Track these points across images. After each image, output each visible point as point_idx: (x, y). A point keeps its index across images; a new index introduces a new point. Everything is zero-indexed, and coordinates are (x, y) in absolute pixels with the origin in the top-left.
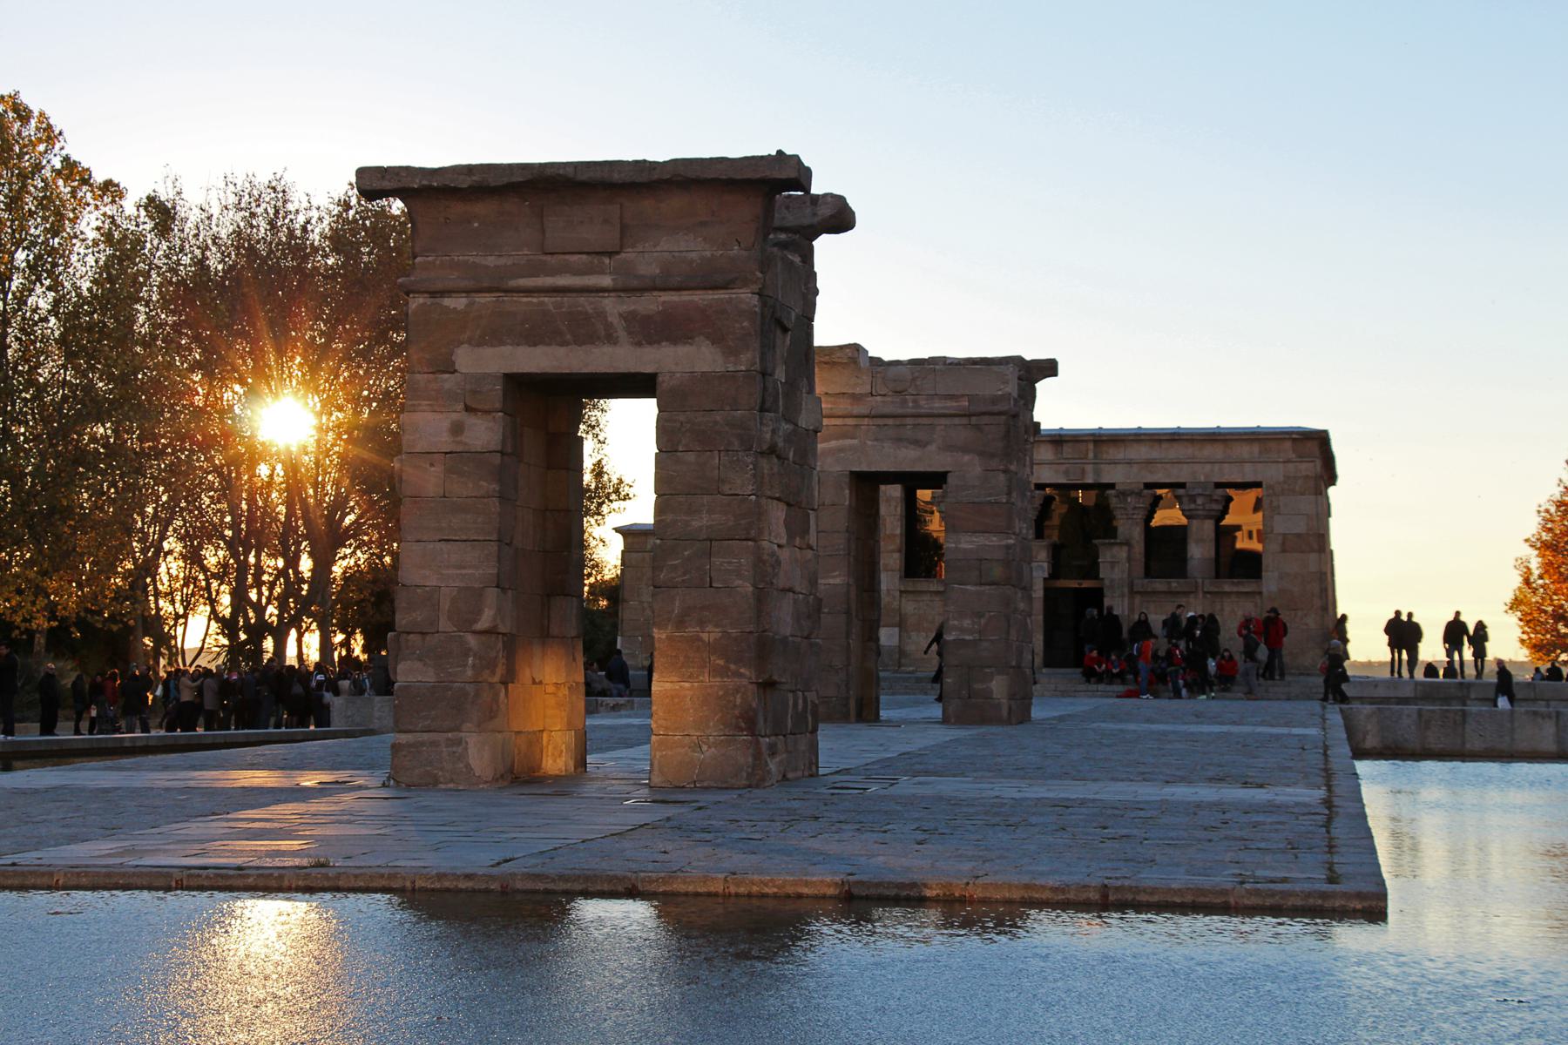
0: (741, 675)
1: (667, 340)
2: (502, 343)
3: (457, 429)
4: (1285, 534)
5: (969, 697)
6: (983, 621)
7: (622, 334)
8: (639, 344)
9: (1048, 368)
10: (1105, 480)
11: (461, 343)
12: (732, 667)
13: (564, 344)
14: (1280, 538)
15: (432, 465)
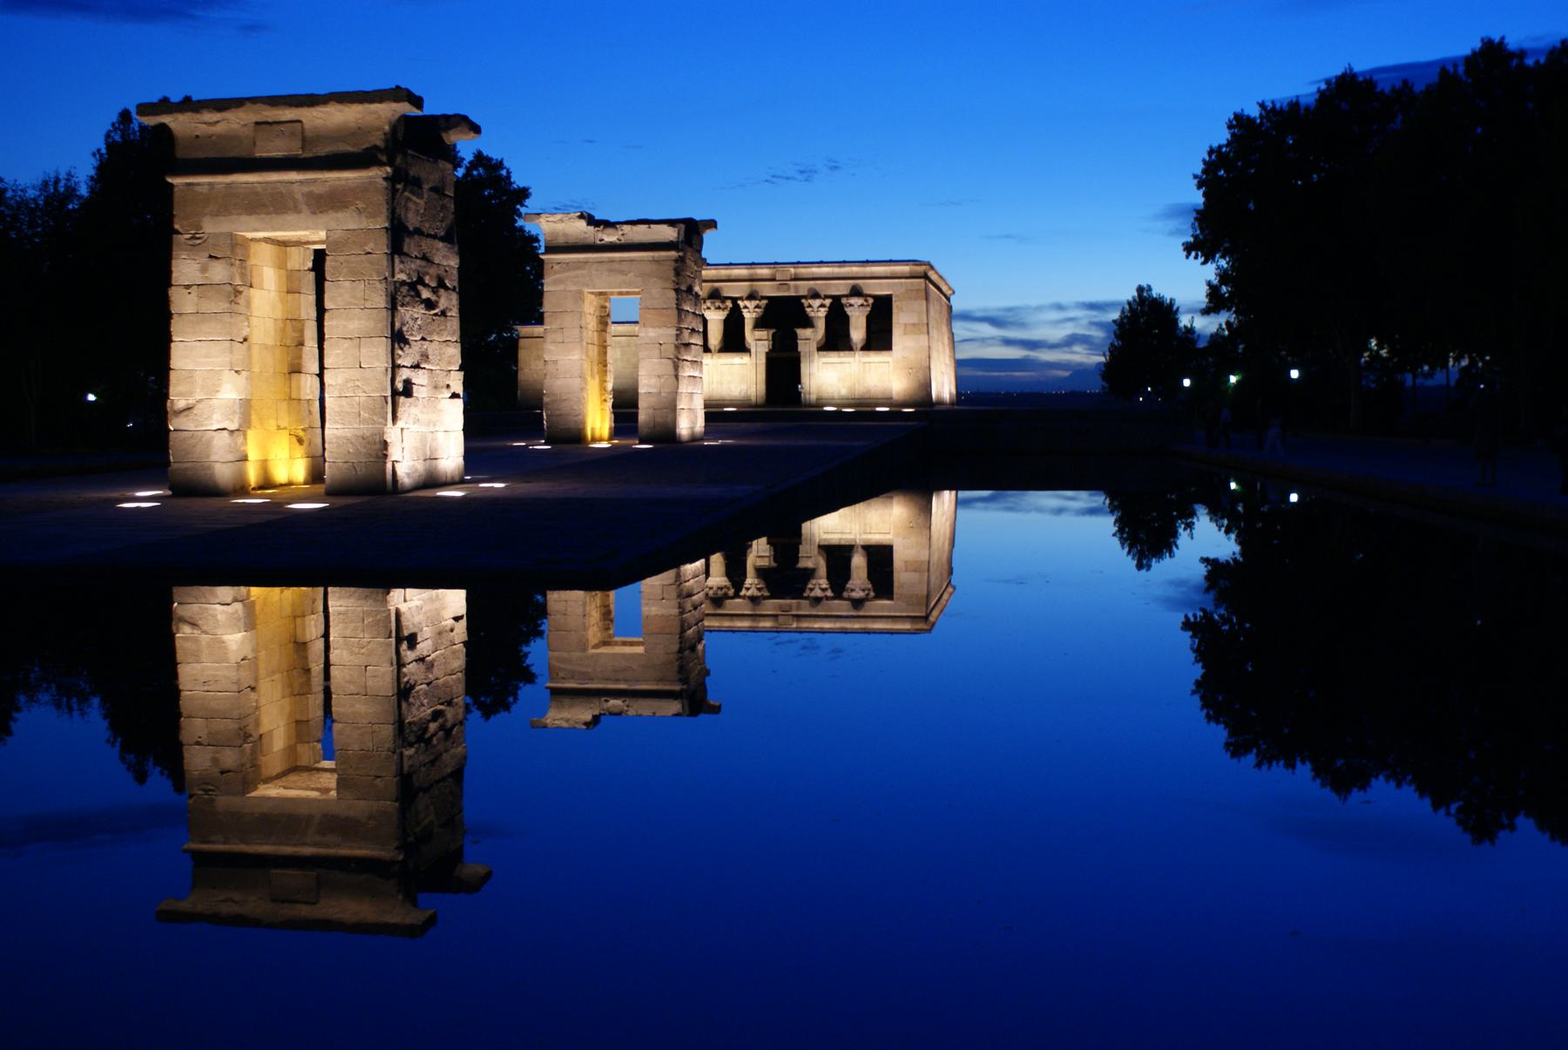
0: (380, 423)
1: (332, 208)
2: (232, 214)
3: (204, 269)
4: (905, 325)
5: (654, 427)
6: (662, 380)
7: (304, 208)
8: (314, 213)
9: (712, 224)
10: (801, 294)
11: (206, 214)
12: (375, 418)
13: (268, 213)
14: (903, 328)
15: (189, 293)
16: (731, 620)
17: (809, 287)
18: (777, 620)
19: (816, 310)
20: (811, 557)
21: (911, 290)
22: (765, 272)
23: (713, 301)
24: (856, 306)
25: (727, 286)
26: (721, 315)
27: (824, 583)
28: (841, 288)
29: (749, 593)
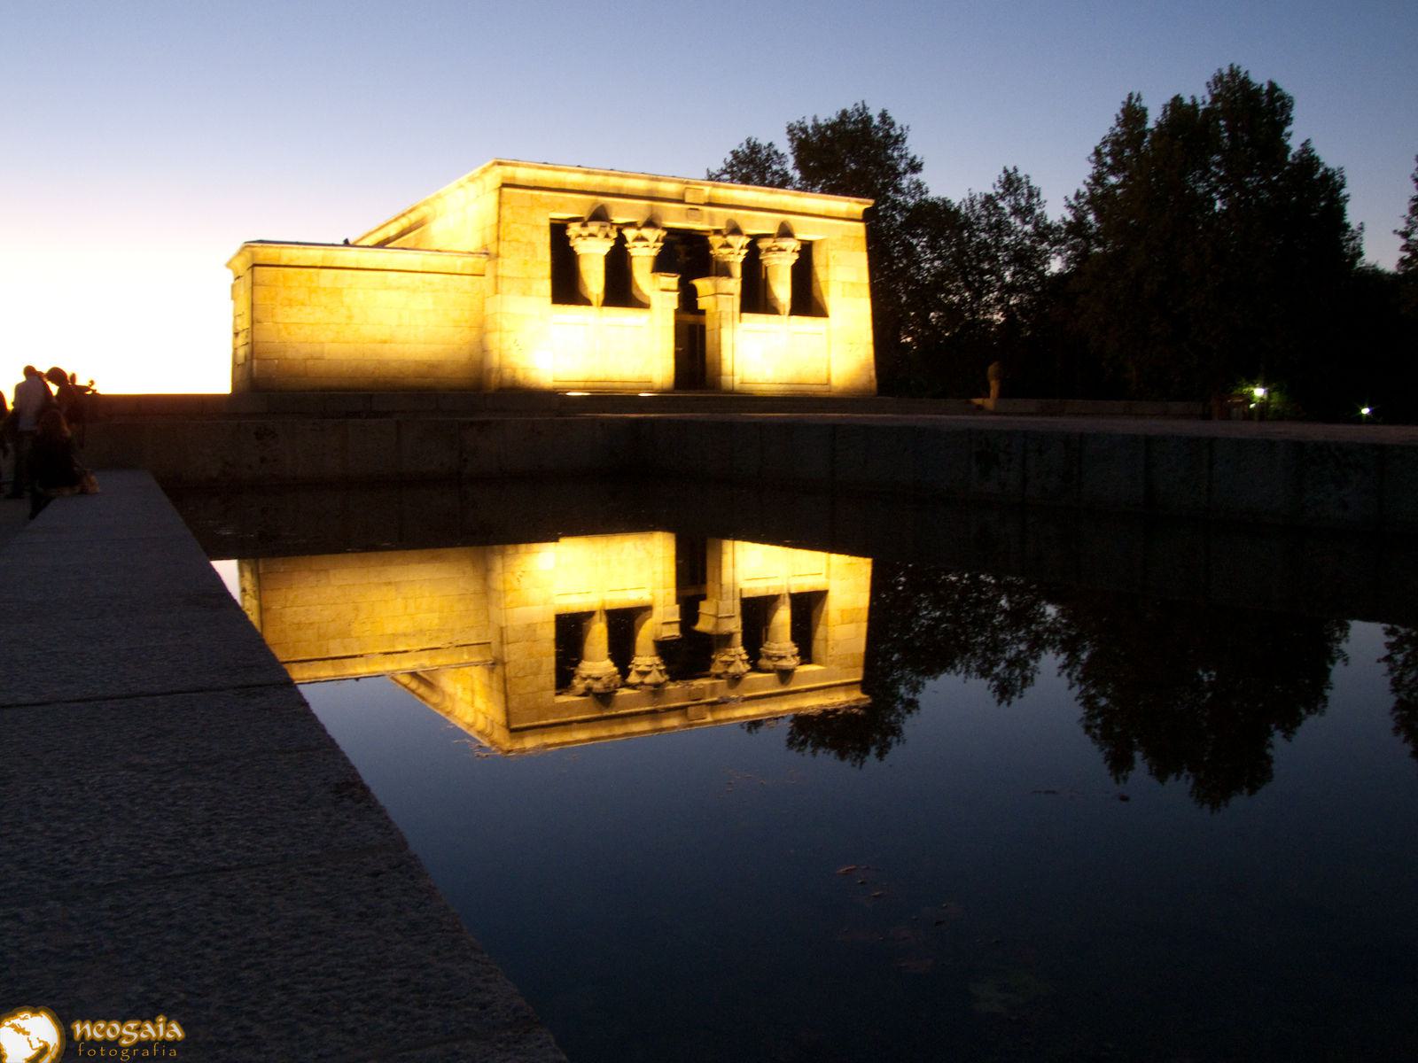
4: (844, 283)
10: (721, 226)
16: (624, 723)
17: (727, 218)
18: (685, 714)
19: (737, 251)
20: (733, 617)
21: (850, 237)
22: (670, 188)
23: (603, 223)
24: (789, 251)
25: (618, 204)
26: (606, 245)
27: (741, 650)
28: (765, 224)
29: (648, 680)
